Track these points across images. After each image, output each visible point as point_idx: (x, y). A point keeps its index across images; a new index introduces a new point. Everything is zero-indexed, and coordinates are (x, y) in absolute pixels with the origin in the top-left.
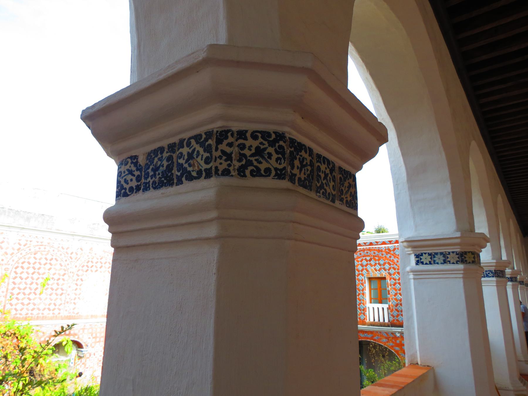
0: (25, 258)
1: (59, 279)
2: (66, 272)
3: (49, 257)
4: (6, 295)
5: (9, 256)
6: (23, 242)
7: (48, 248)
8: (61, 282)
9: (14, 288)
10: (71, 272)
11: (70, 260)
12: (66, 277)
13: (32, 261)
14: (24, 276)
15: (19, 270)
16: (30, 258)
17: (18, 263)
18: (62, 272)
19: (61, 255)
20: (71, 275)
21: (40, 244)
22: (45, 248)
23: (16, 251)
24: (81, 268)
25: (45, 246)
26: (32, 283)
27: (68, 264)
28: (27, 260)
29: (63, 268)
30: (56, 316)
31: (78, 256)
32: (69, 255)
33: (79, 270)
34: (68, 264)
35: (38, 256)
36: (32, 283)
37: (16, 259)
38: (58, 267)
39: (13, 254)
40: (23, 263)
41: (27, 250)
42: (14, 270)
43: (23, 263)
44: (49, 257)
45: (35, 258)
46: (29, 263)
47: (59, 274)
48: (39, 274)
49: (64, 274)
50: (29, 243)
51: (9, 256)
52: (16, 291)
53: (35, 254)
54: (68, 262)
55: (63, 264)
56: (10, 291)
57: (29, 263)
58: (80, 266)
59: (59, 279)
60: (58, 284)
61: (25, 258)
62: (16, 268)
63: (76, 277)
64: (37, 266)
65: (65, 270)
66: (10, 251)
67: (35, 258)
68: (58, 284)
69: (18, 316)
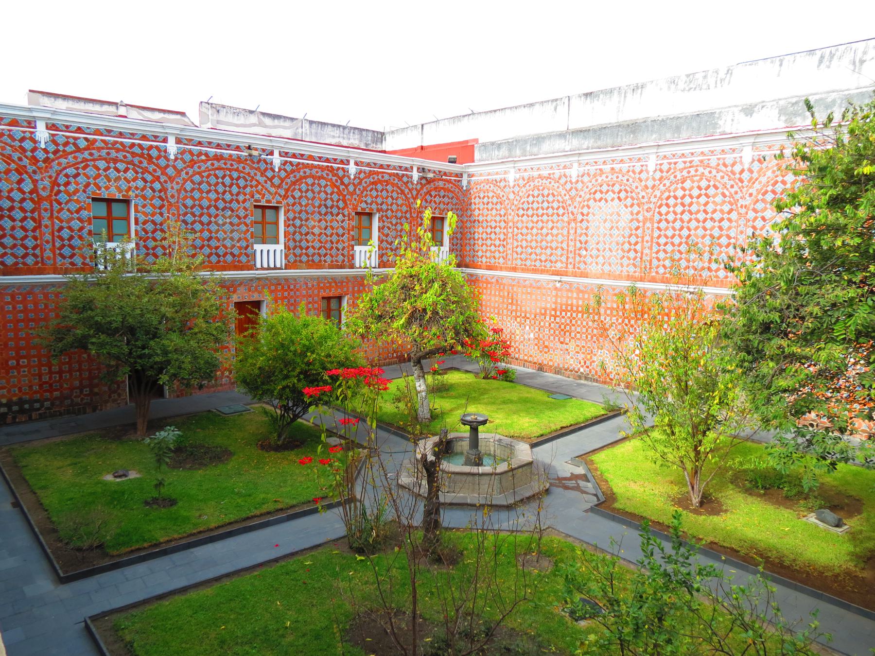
0: (670, 191)
1: (721, 220)
2: (734, 207)
3: (704, 184)
4: (652, 245)
5: (650, 190)
6: (665, 167)
7: (701, 170)
8: (725, 224)
9: (659, 237)
10: (742, 206)
11: (740, 184)
12: (734, 216)
13: (680, 193)
14: (671, 217)
15: (664, 210)
16: (676, 190)
17: (662, 200)
18: (726, 208)
19: (722, 177)
20: (743, 211)
21: (688, 165)
22: (696, 171)
23: (658, 182)
24: (760, 197)
25: (697, 166)
26: (682, 228)
27: (736, 193)
28: (672, 194)
29: (727, 199)
30: (722, 281)
31: (755, 175)
32: (738, 176)
33: (757, 201)
34: (736, 193)
35: (687, 185)
36: (682, 228)
37: (658, 193)
38: (719, 199)
39: (654, 186)
40: (668, 198)
41: (672, 177)
42: (657, 210)
43: (668, 198)
44: (704, 184)
45: (683, 189)
46: (676, 198)
47: (722, 211)
48: (690, 213)
49: (730, 212)
50: (672, 166)
51: (650, 190)
52: (662, 240)
53: (682, 183)
54: (736, 188)
55: (727, 193)
56: (655, 240)
57: (676, 198)
58: (758, 194)
59: (721, 220)
60: (721, 228)
61: (670, 191)
62: (660, 207)
63: (751, 215)
64: (687, 200)
65: (732, 205)
66: (650, 183)
67: (683, 189)
68: (721, 228)
69: (668, 275)
